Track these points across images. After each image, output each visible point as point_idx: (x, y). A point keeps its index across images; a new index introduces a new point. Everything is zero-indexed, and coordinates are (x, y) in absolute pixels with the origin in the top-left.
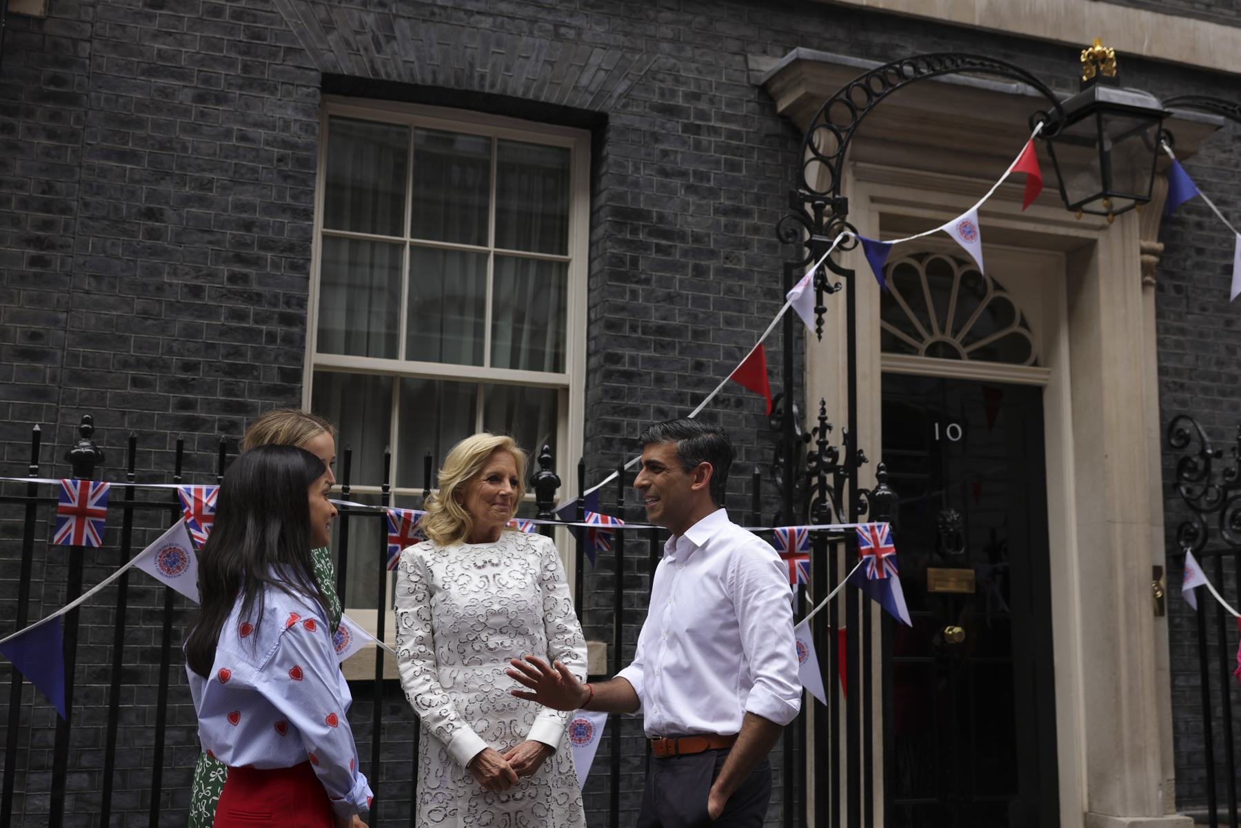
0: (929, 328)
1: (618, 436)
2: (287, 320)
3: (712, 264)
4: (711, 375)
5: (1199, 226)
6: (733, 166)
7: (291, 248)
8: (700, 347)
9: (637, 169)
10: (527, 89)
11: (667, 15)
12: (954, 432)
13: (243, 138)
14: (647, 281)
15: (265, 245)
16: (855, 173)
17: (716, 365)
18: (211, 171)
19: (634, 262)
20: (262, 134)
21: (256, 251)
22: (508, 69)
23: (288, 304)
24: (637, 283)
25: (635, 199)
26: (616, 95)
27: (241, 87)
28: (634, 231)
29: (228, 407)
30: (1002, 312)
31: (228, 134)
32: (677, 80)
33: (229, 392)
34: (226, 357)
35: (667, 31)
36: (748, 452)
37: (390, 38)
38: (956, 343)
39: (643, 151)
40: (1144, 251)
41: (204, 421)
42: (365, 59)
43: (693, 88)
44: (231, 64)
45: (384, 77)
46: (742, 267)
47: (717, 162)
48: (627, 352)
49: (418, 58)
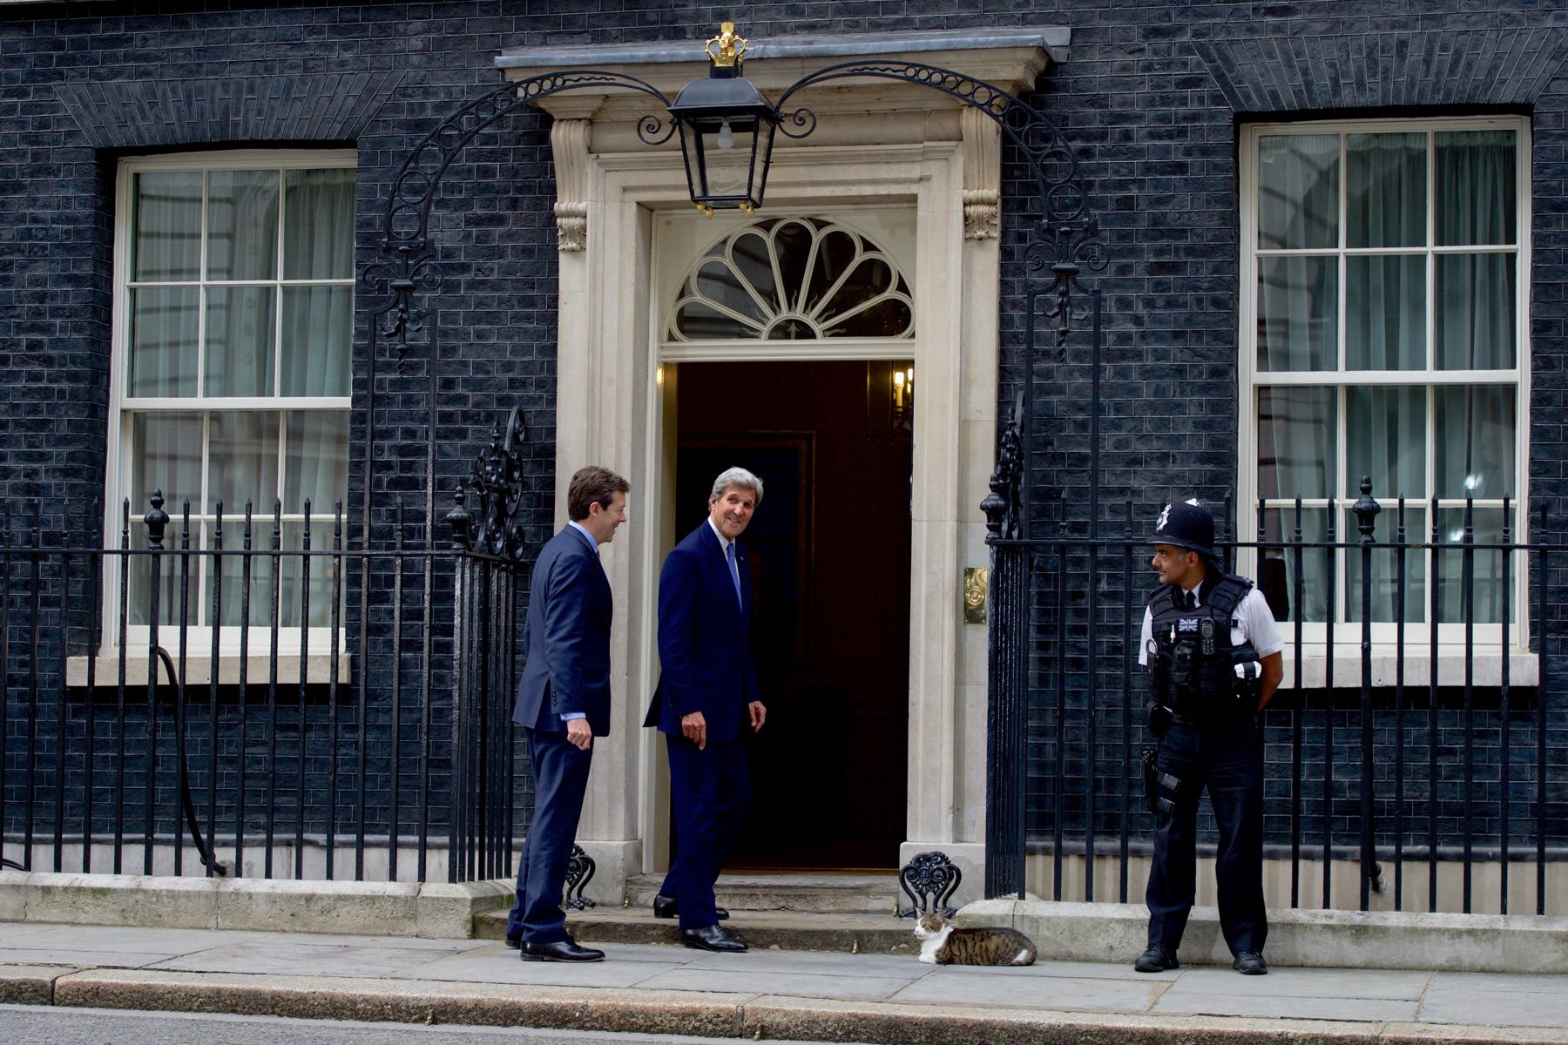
2: (73, 377)
3: (464, 278)
4: (460, 391)
5: (1086, 153)
6: (485, 172)
7: (74, 313)
8: (448, 364)
10: (279, 130)
11: (418, 25)
13: (35, 220)
15: (55, 312)
17: (465, 380)
18: (11, 253)
20: (48, 213)
21: (48, 320)
22: (259, 113)
23: (74, 364)
26: (363, 119)
27: (32, 175)
29: (29, 457)
30: (875, 275)
31: (21, 219)
32: (427, 92)
33: (31, 445)
34: (28, 414)
35: (416, 43)
37: (153, 105)
38: (809, 319)
41: (13, 471)
42: (132, 129)
43: (442, 97)
44: (23, 155)
45: (148, 142)
46: (494, 276)
47: (470, 171)
49: (179, 119)
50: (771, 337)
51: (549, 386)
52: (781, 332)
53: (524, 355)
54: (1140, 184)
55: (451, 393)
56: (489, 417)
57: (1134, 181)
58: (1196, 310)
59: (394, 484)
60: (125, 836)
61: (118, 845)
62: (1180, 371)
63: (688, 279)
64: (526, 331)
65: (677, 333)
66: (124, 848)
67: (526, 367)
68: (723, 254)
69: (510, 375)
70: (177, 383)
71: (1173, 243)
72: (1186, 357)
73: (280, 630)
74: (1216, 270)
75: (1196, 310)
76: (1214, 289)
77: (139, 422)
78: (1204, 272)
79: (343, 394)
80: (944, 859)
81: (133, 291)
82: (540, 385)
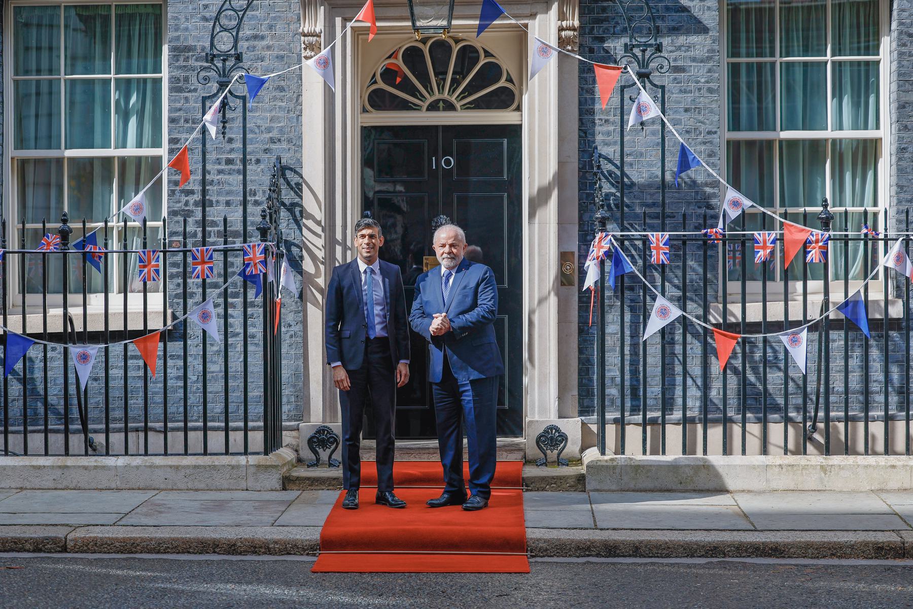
0: (455, 83)
1: (178, 188)
9: (187, 19)
12: (448, 162)
14: (195, 90)
16: (329, 4)
19: (186, 79)
24: (189, 92)
25: (186, 39)
28: (187, 59)
30: (492, 72)
36: (264, 192)
38: (453, 99)
39: (190, 8)
40: (561, 29)
48: (184, 136)
50: (428, 109)
51: (296, 143)
52: (433, 107)
53: (280, 122)
54: (663, 18)
55: (234, 146)
56: (258, 161)
57: (659, 17)
58: (697, 95)
59: (196, 204)
60: (29, 428)
61: (25, 432)
62: (687, 132)
63: (374, 75)
64: (280, 107)
65: (368, 107)
66: (29, 435)
67: (281, 130)
68: (396, 58)
69: (271, 135)
70: (51, 142)
71: (683, 54)
72: (691, 123)
73: (129, 294)
74: (709, 71)
75: (697, 95)
76: (707, 82)
77: (23, 164)
78: (703, 71)
79: (156, 144)
80: (557, 430)
81: (16, 83)
82: (289, 141)
